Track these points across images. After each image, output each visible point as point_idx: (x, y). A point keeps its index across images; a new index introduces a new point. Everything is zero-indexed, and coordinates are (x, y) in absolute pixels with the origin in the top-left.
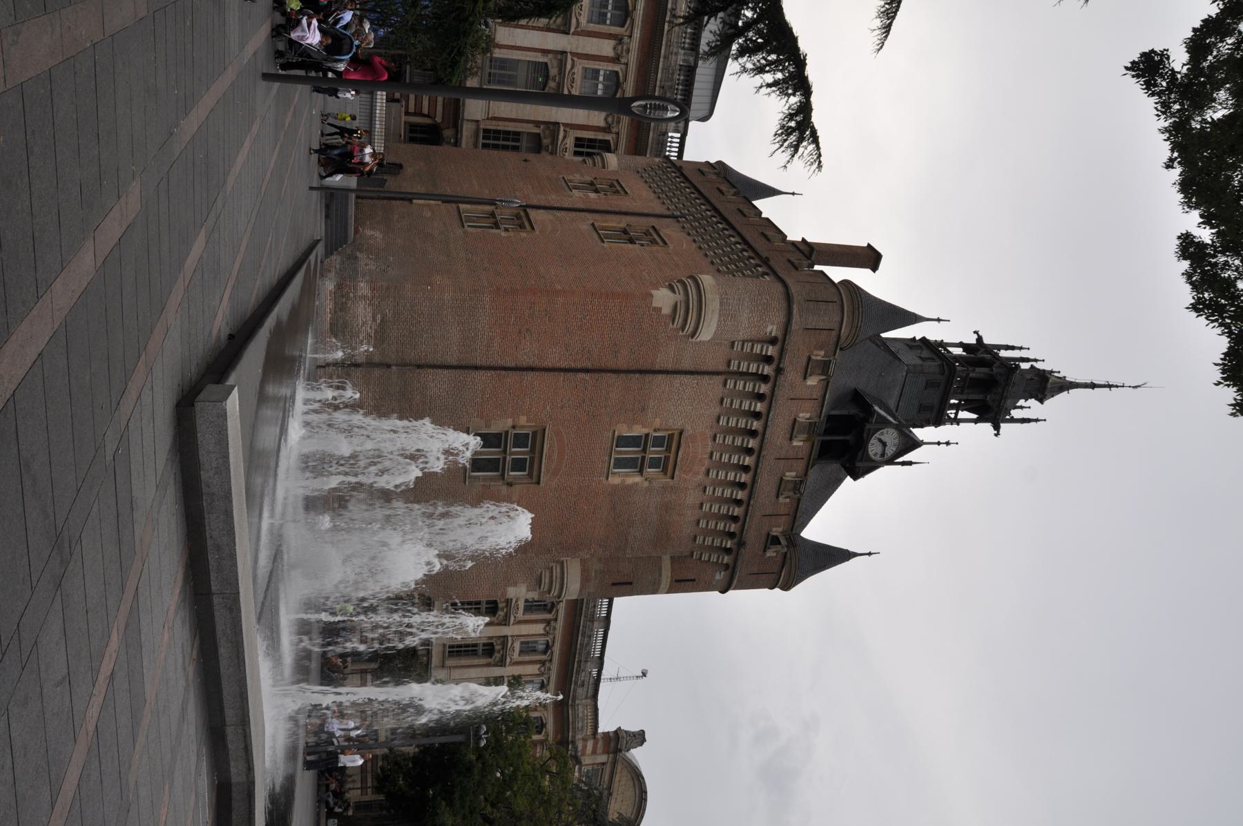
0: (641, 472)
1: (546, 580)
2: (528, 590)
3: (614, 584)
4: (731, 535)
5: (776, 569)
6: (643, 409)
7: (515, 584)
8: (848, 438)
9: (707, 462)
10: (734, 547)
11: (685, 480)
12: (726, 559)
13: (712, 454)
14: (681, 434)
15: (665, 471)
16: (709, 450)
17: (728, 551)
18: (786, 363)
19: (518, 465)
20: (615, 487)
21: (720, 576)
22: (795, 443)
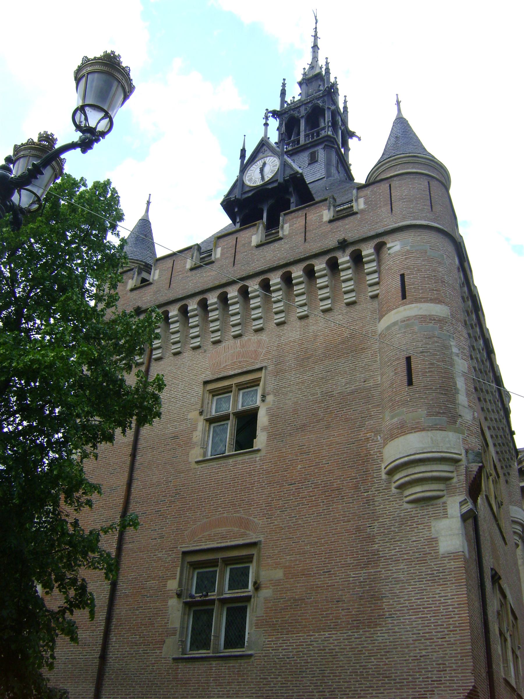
1: (417, 491)
2: (445, 515)
3: (410, 383)
5: (384, 186)
6: (176, 437)
7: (433, 541)
9: (245, 338)
10: (349, 251)
11: (268, 352)
12: (368, 250)
13: (235, 337)
14: (206, 383)
15: (256, 383)
16: (232, 341)
19: (239, 579)
20: (271, 437)
21: (395, 246)
22: (218, 255)
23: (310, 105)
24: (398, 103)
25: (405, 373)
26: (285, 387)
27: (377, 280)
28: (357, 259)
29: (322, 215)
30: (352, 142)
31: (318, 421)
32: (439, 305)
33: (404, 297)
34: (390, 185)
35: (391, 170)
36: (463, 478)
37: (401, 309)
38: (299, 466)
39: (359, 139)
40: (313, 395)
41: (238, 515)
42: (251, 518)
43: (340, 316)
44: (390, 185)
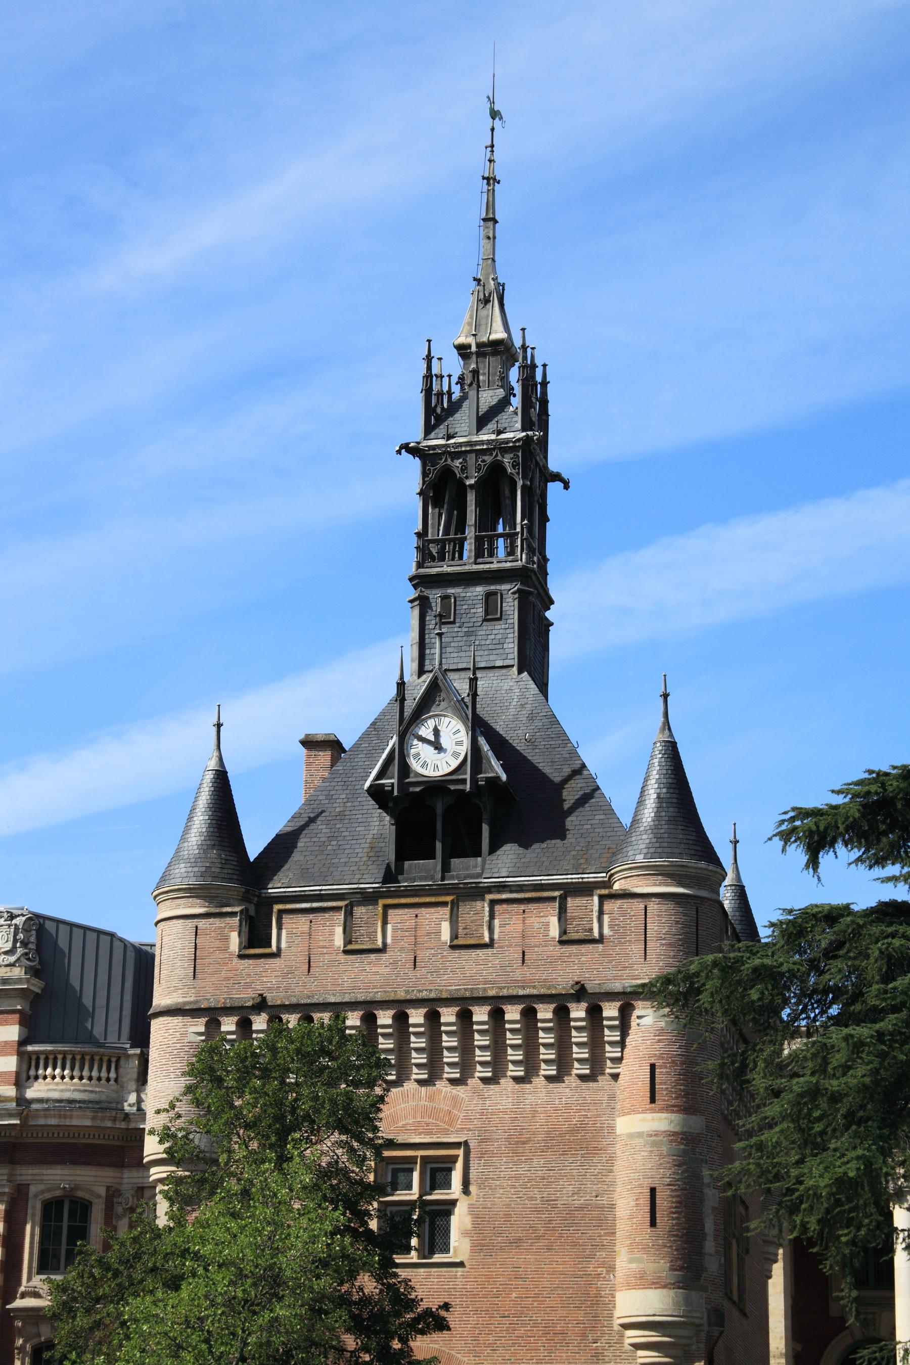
0: (454, 1203)
3: (653, 1223)
4: (562, 1013)
5: (639, 905)
8: (439, 810)
11: (468, 1119)
12: (610, 1010)
17: (595, 1012)
18: (247, 996)
23: (489, 459)
24: (665, 696)
25: (647, 1209)
26: (493, 1179)
27: (619, 1055)
28: (595, 1012)
29: (547, 924)
30: (553, 488)
31: (538, 1238)
32: (694, 1117)
33: (653, 1100)
34: (646, 907)
35: (649, 880)
36: (702, 1345)
37: (649, 1116)
38: (514, 1295)
39: (566, 486)
40: (532, 1199)
41: (436, 1346)
42: (453, 1352)
43: (567, 1090)
44: (646, 907)
